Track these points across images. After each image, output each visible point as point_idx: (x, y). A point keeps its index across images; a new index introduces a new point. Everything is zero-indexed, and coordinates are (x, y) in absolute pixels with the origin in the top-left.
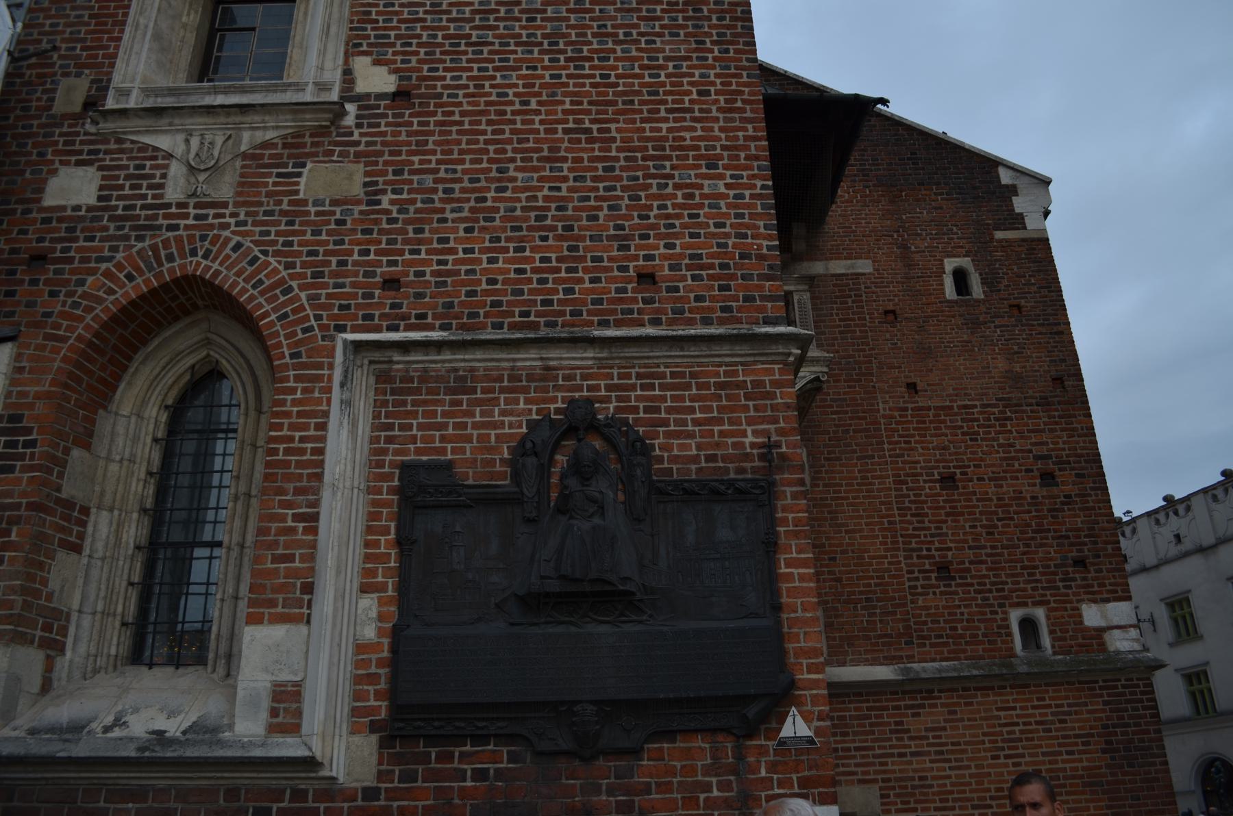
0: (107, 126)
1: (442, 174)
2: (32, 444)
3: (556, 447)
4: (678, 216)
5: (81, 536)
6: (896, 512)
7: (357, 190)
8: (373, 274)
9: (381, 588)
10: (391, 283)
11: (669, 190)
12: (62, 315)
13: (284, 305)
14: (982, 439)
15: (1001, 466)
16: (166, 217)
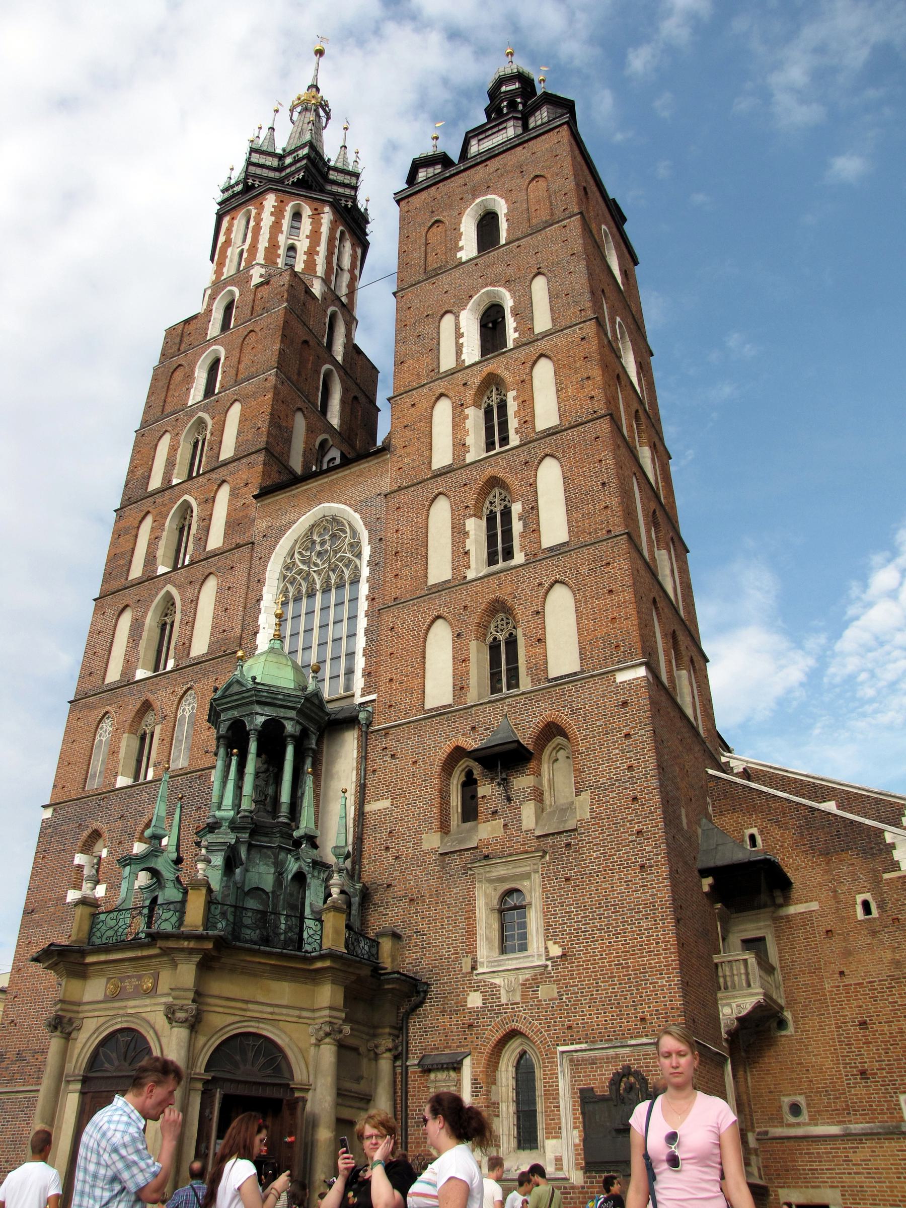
0: (479, 977)
1: (579, 987)
2: (481, 1087)
3: (621, 1080)
4: (651, 995)
5: (499, 1112)
6: (837, 1043)
7: (556, 995)
8: (563, 1025)
9: (579, 1127)
10: (570, 1027)
11: (648, 985)
12: (481, 1045)
13: (541, 1037)
14: (880, 1000)
15: (891, 1014)
16: (503, 1009)
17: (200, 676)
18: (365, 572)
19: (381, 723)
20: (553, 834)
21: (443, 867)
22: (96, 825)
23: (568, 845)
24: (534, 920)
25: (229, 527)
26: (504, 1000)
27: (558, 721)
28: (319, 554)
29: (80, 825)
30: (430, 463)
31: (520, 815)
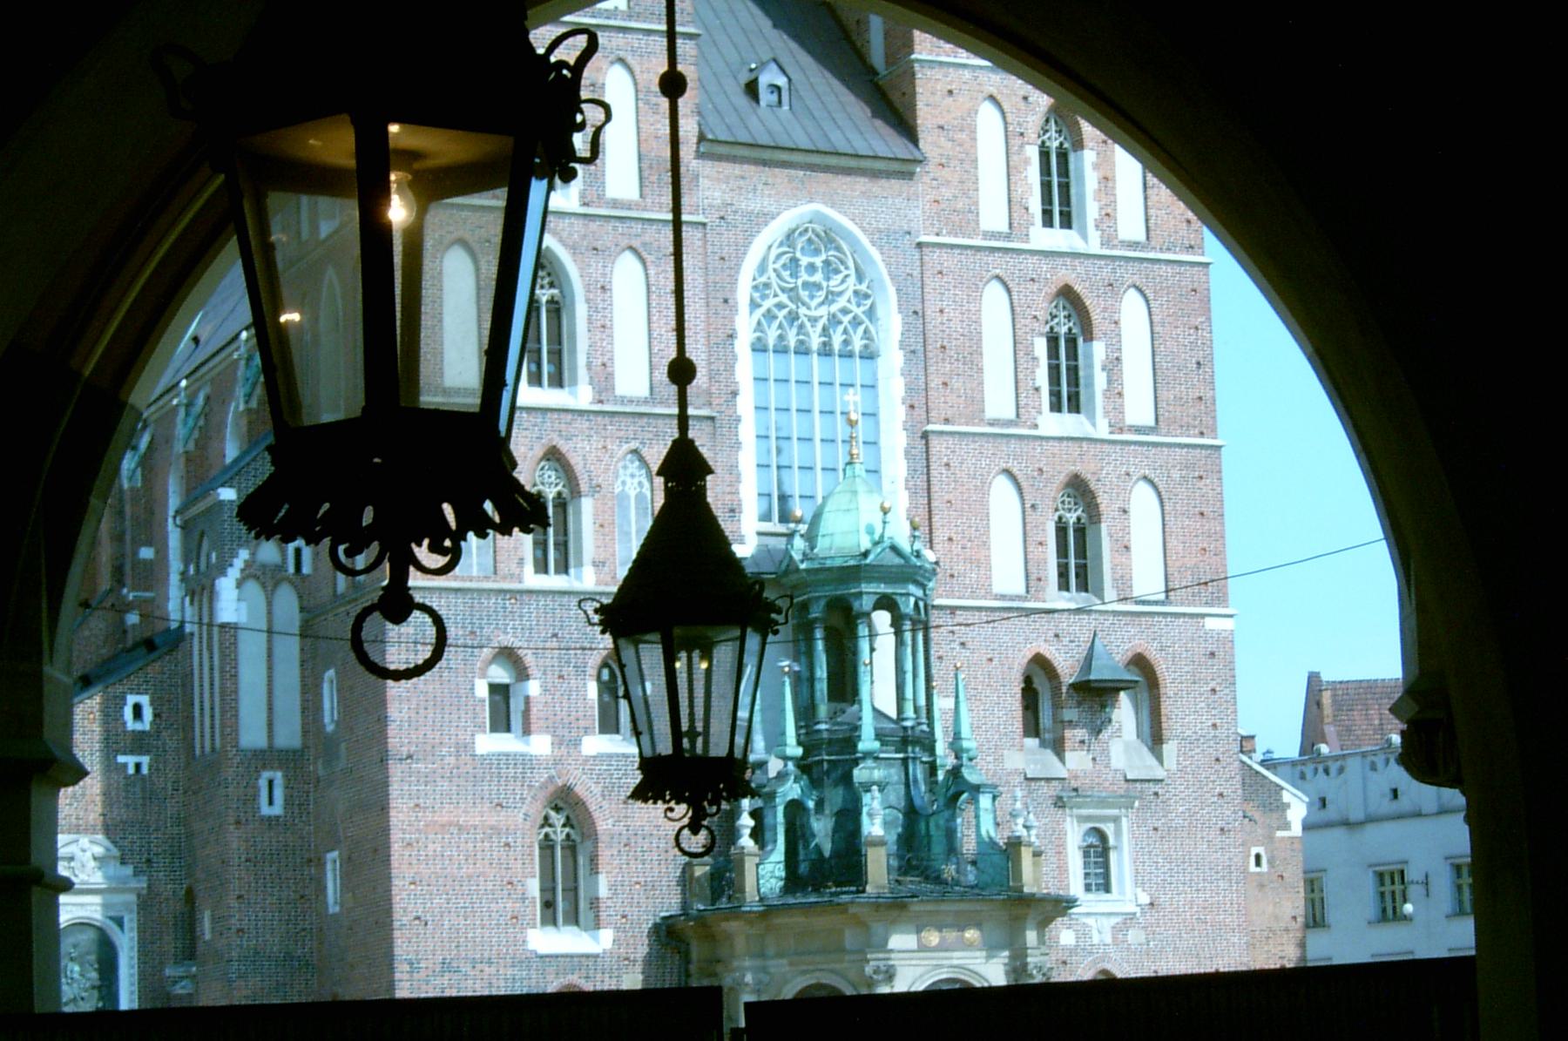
7: (1144, 941)
17: (651, 436)
18: (892, 360)
19: (941, 596)
20: (1142, 781)
21: (1029, 793)
22: (508, 640)
23: (1156, 794)
24: (1122, 864)
25: (651, 167)
26: (1096, 940)
27: (1147, 654)
28: (806, 285)
29: (472, 633)
30: (978, 213)
31: (1108, 749)
